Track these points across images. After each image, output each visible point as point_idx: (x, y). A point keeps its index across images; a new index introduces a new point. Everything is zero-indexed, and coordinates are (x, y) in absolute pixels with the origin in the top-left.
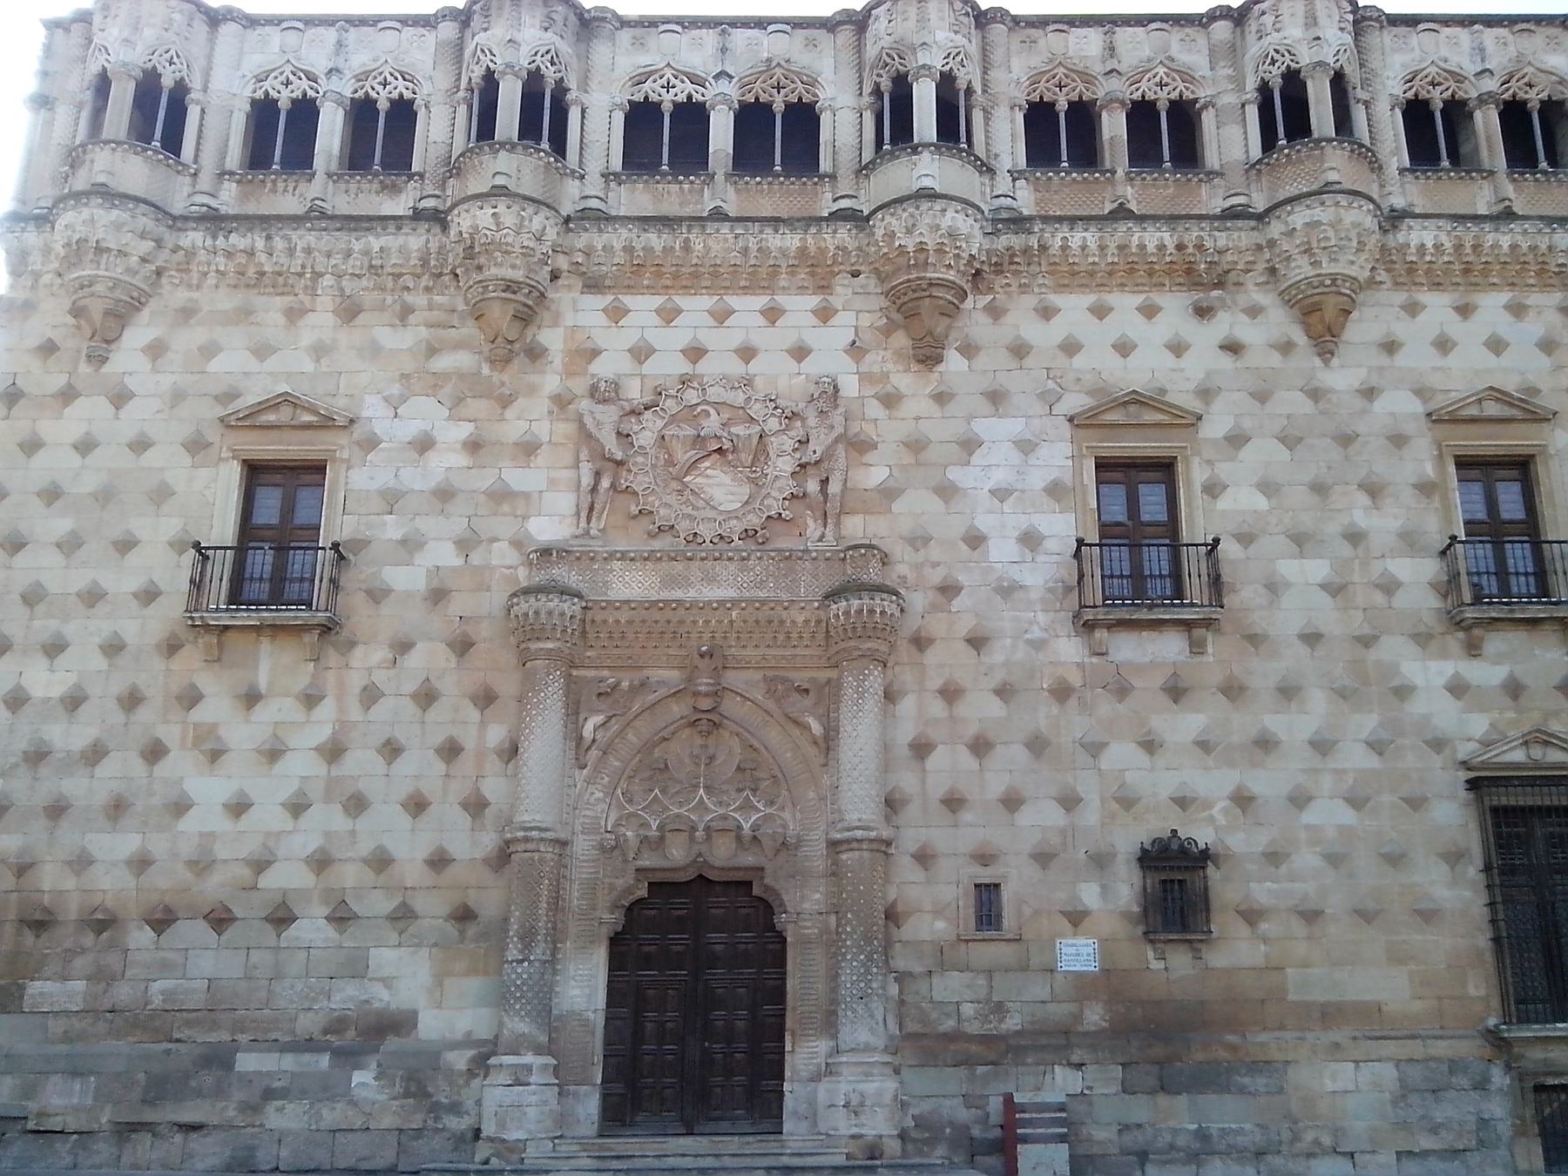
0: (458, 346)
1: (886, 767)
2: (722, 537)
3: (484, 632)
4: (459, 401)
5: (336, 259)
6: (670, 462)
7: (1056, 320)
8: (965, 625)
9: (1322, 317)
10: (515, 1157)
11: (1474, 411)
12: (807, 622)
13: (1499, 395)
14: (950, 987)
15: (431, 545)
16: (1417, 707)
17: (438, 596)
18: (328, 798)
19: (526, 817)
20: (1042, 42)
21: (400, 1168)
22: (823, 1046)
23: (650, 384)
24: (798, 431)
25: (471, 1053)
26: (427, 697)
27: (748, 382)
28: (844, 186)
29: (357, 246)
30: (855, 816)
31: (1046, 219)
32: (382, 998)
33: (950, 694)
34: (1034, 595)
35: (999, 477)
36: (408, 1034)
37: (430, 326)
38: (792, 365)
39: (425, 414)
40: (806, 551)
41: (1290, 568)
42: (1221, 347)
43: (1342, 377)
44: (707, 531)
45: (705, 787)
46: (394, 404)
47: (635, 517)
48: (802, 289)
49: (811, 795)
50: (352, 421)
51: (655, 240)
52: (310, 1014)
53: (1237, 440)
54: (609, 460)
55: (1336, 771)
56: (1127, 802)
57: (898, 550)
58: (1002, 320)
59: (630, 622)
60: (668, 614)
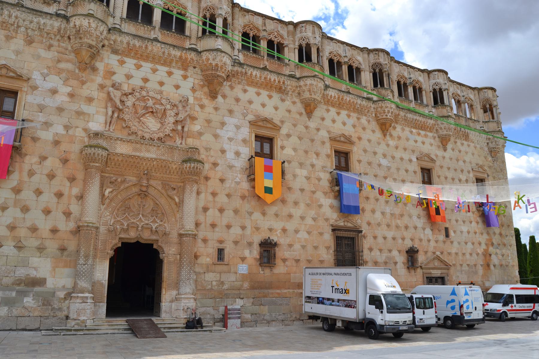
0: (68, 61)
1: (196, 213)
2: (151, 139)
3: (73, 157)
4: (67, 79)
5: (27, 23)
6: (136, 112)
7: (247, 93)
8: (219, 175)
9: (309, 108)
10: (84, 325)
11: (338, 139)
12: (176, 168)
13: (344, 135)
14: (210, 277)
15: (55, 125)
16: (323, 210)
17: (57, 143)
18: (15, 206)
19: (87, 219)
20: (247, 16)
21: (41, 328)
22: (174, 293)
23: (131, 87)
24: (175, 110)
25: (65, 293)
26: (51, 176)
27: (161, 92)
28: (193, 41)
29: (35, 20)
30: (189, 227)
31: (248, 65)
32: (33, 274)
33: (214, 194)
34: (238, 169)
35: (230, 134)
36: (43, 286)
37: (58, 52)
38: (175, 90)
39: (54, 81)
40: (177, 147)
41: (298, 171)
42: (286, 111)
43: (312, 124)
44: (147, 136)
45: (143, 215)
46: (45, 77)
47: (124, 128)
48: (179, 68)
50: (29, 79)
51: (137, 43)
52: (8, 278)
53: (289, 136)
54: (117, 108)
55: (305, 225)
56: (257, 229)
57: (202, 151)
59: (122, 161)
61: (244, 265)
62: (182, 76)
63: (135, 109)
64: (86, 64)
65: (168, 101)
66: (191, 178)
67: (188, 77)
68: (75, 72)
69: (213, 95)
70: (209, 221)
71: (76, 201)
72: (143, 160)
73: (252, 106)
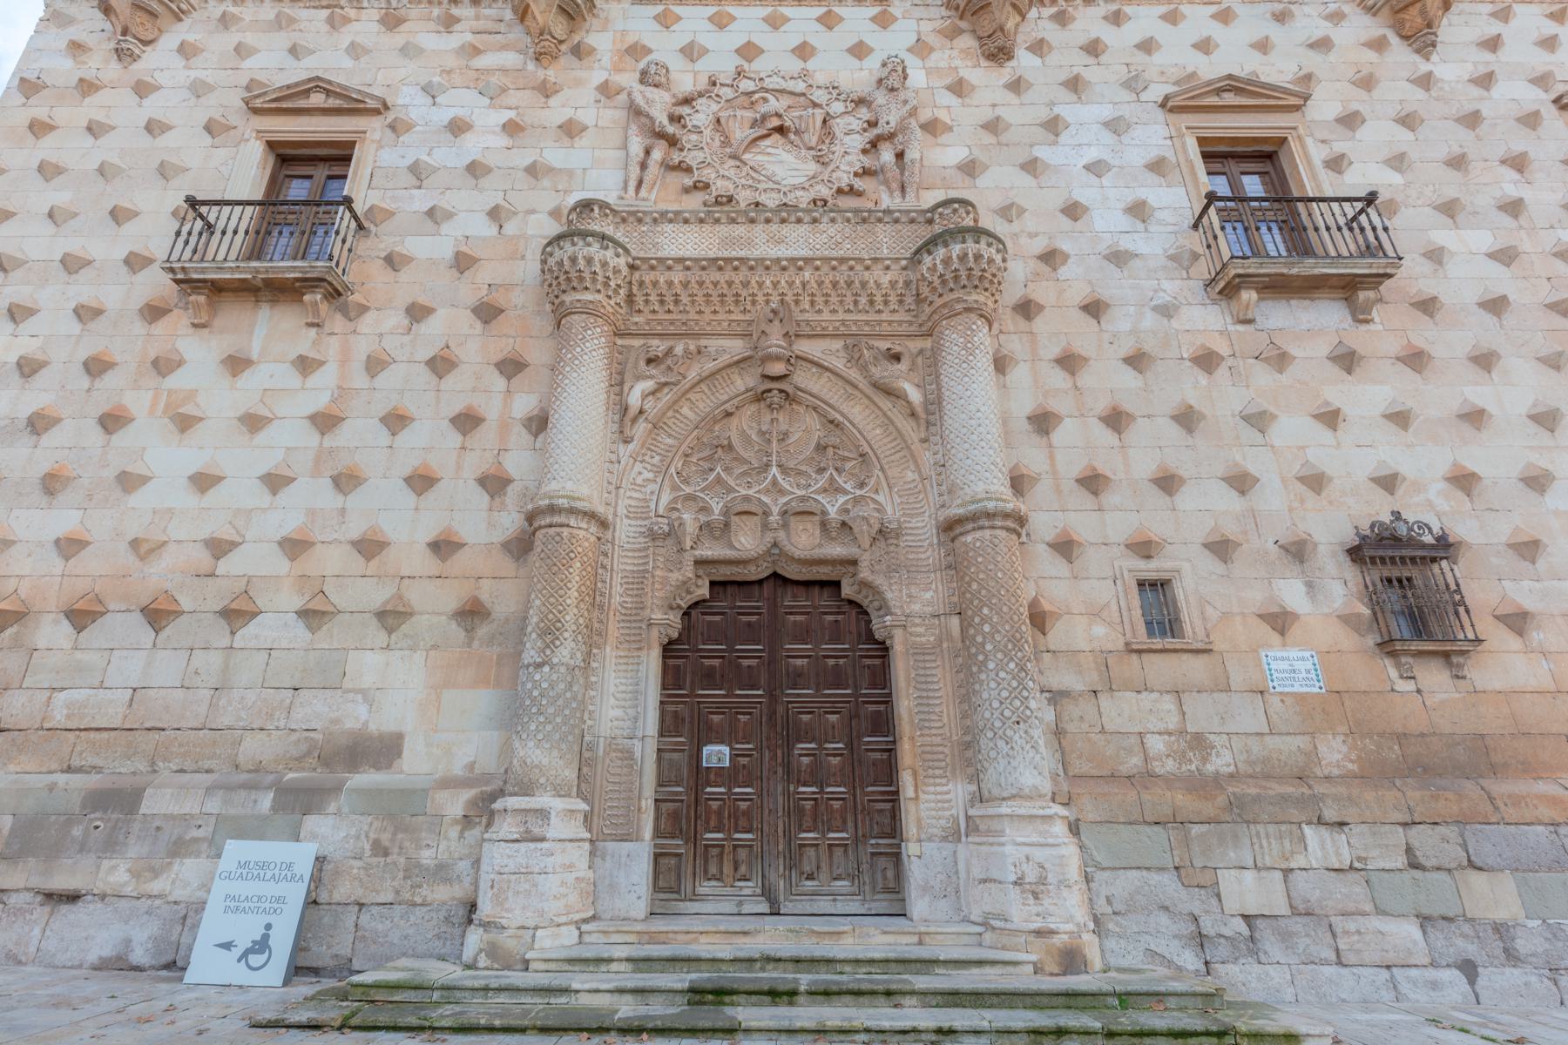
0: (504, 47)
6: (726, 142)
8: (1078, 293)
17: (463, 263)
26: (441, 365)
35: (1092, 154)
38: (855, 62)
39: (461, 101)
44: (771, 200)
49: (910, 476)
58: (1070, 27)
59: (685, 285)
60: (729, 274)
61: (1294, 653)
62: (873, 19)
63: (723, 133)
64: (561, 42)
65: (834, 92)
66: (959, 300)
67: (897, 19)
68: (524, 69)
69: (998, 53)
70: (1070, 466)
71: (526, 437)
72: (760, 270)
73: (1158, 58)
